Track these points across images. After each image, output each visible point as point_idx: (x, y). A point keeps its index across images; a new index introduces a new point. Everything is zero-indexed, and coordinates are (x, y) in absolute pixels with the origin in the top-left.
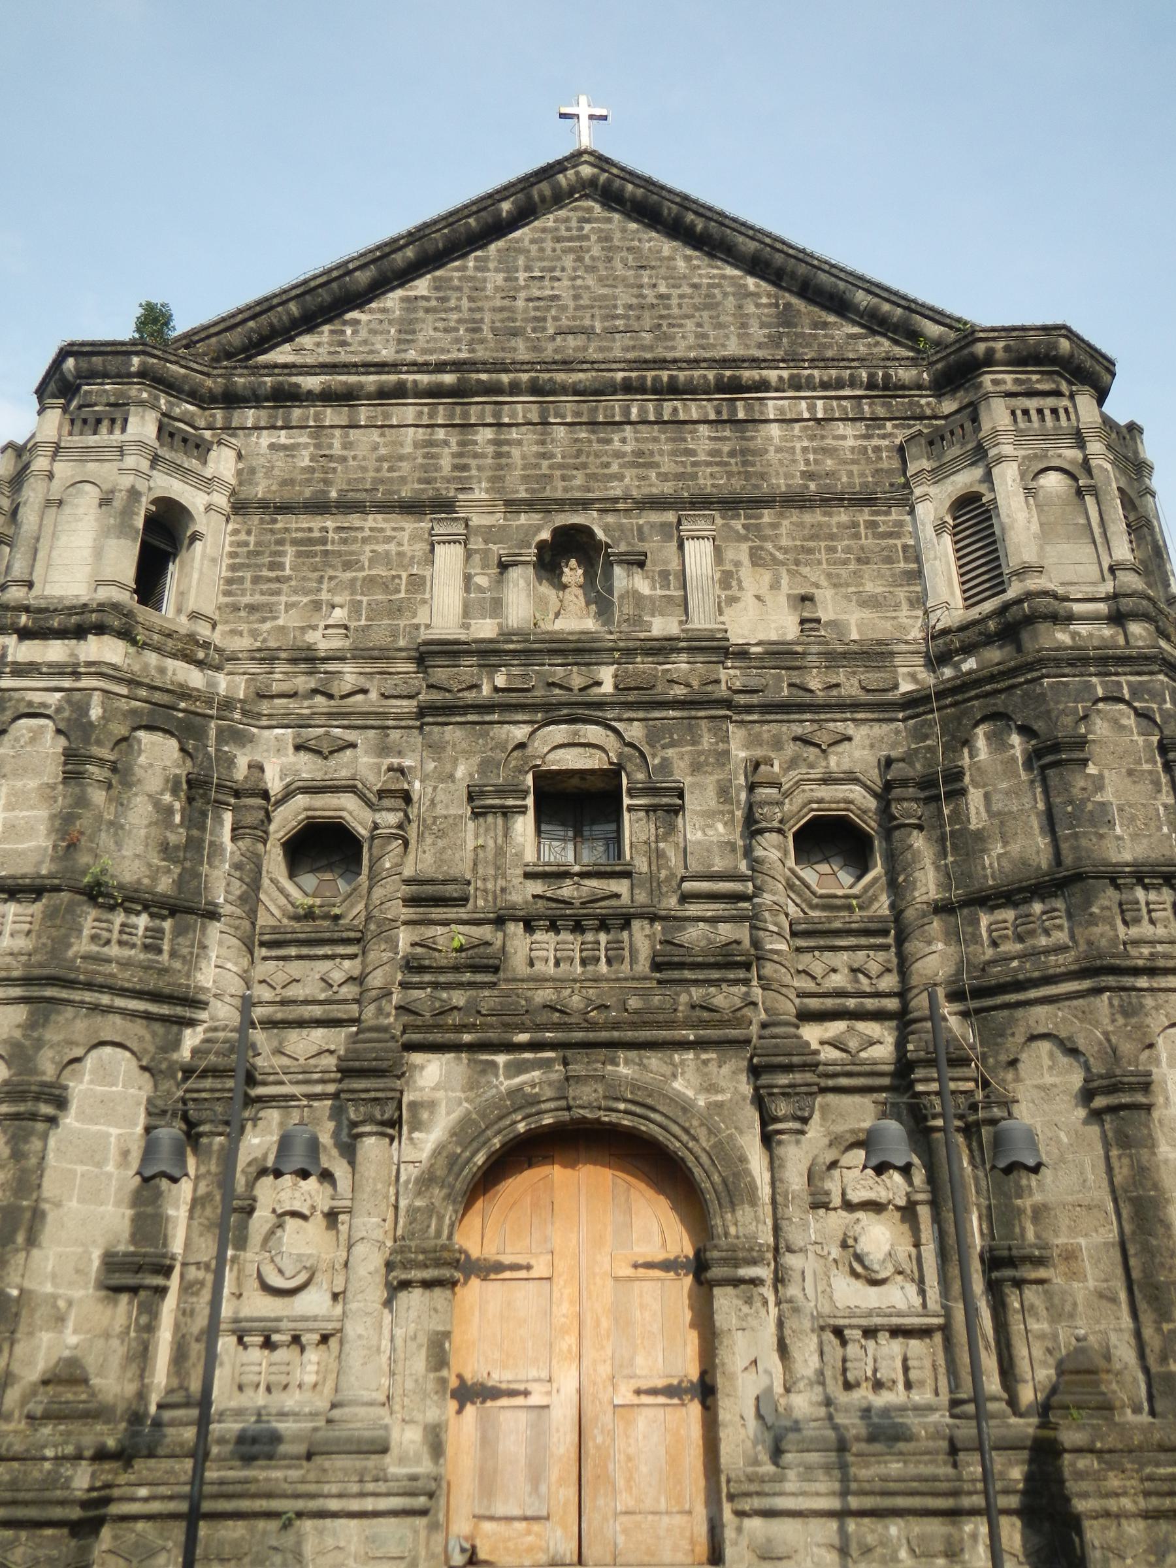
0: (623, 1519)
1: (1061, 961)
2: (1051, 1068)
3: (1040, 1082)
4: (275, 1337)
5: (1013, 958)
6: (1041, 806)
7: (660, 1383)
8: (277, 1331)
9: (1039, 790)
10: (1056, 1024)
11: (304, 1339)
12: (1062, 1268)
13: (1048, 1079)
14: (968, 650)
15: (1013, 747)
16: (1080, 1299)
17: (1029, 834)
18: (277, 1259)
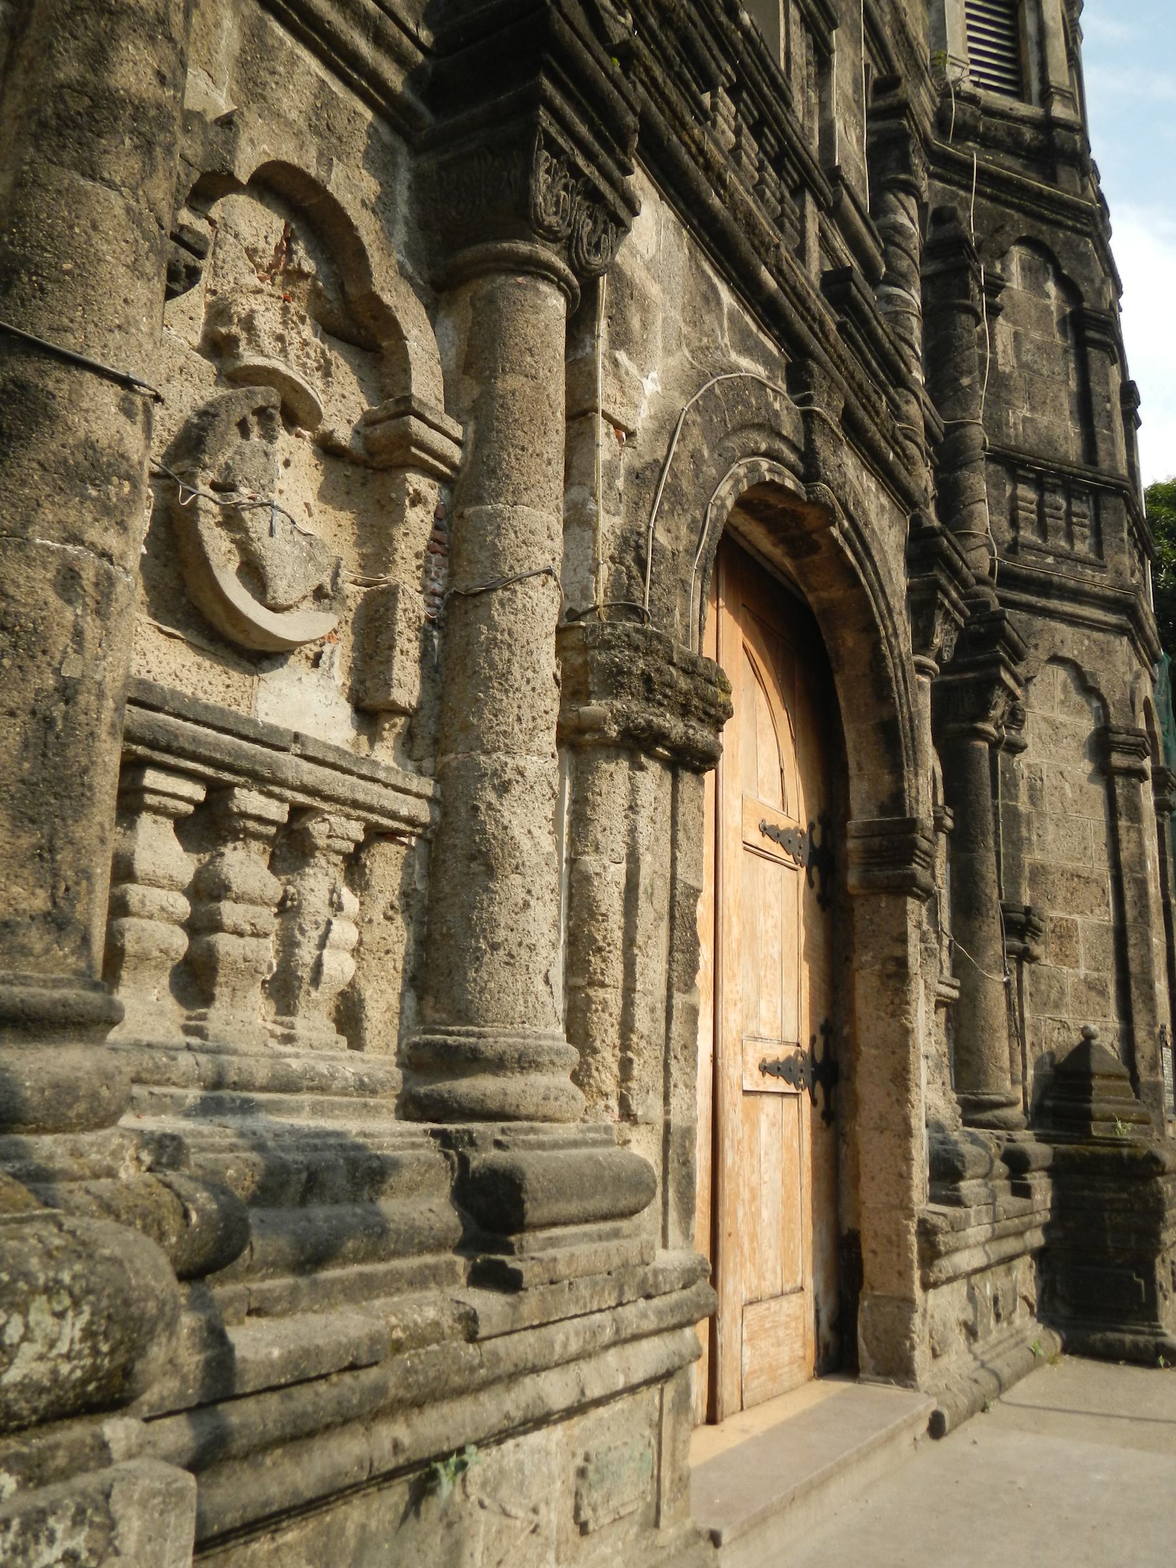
0: (751, 1312)
1: (1097, 579)
2: (1062, 702)
3: (1047, 714)
4: (249, 800)
5: (1049, 553)
6: (1073, 385)
7: (780, 1053)
8: (262, 781)
9: (1072, 365)
10: (1080, 652)
11: (317, 829)
12: (1054, 947)
13: (1061, 717)
14: (988, 142)
15: (1048, 296)
16: (1069, 990)
17: (1057, 410)
18: (257, 523)
